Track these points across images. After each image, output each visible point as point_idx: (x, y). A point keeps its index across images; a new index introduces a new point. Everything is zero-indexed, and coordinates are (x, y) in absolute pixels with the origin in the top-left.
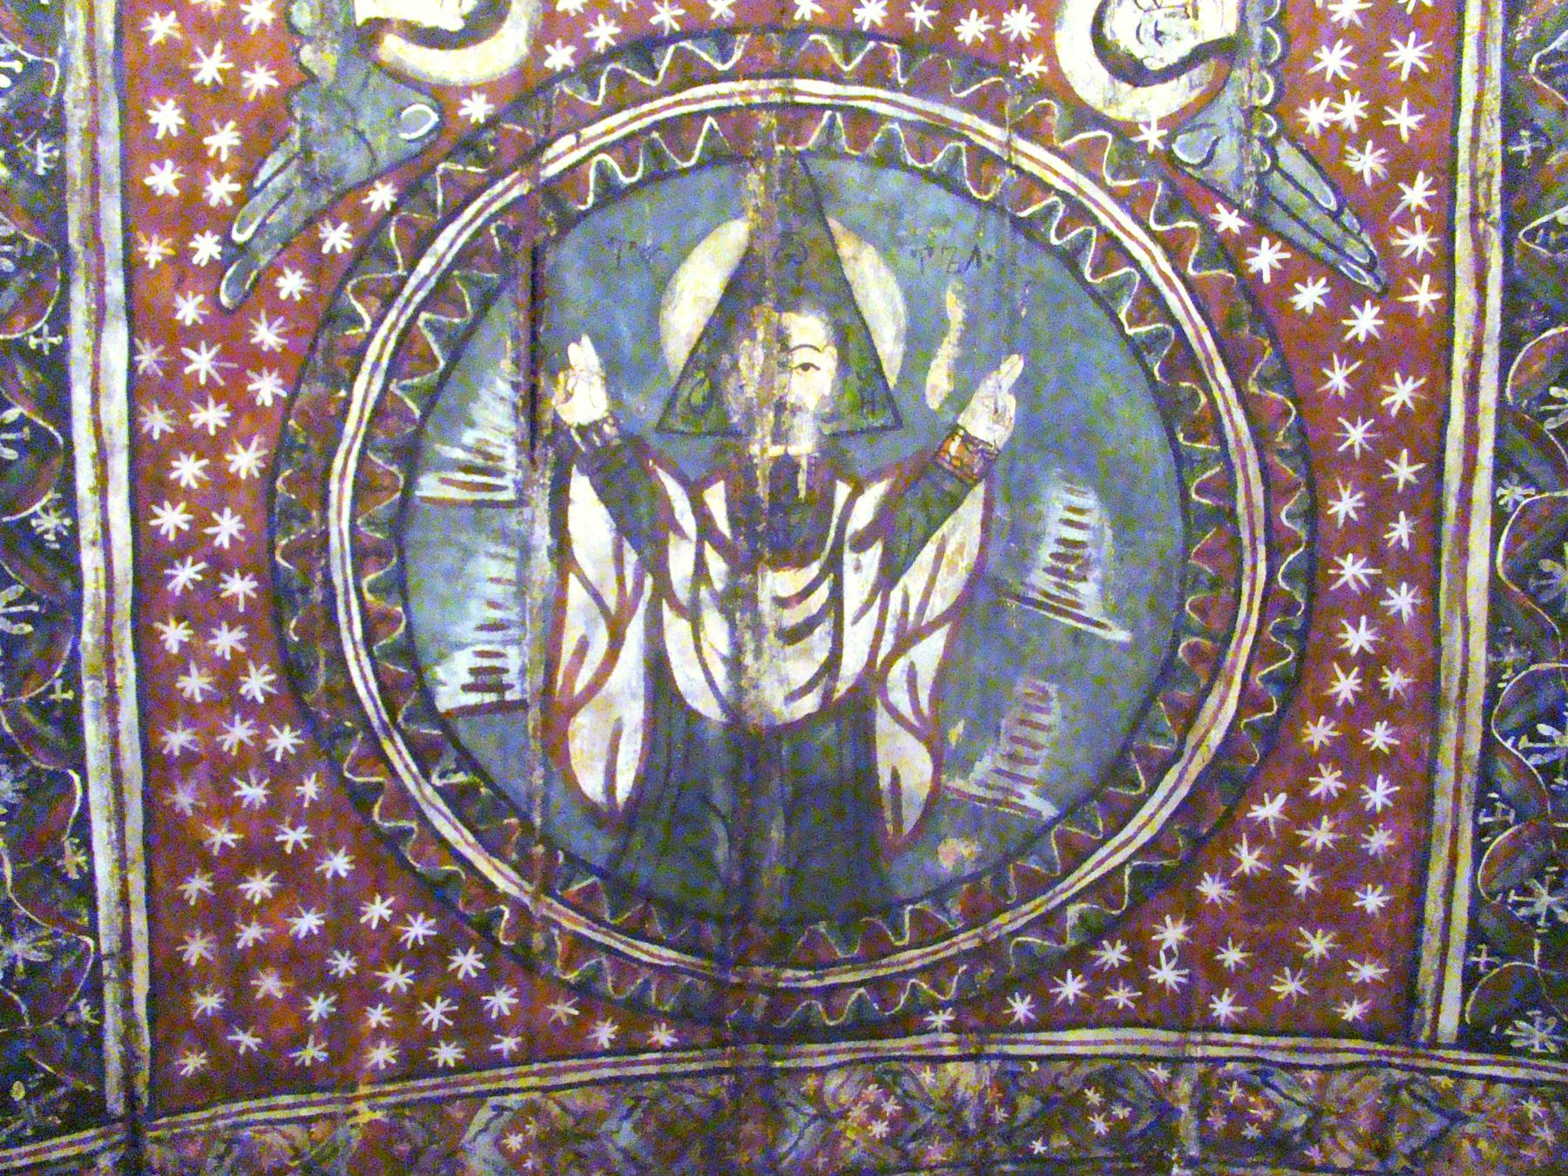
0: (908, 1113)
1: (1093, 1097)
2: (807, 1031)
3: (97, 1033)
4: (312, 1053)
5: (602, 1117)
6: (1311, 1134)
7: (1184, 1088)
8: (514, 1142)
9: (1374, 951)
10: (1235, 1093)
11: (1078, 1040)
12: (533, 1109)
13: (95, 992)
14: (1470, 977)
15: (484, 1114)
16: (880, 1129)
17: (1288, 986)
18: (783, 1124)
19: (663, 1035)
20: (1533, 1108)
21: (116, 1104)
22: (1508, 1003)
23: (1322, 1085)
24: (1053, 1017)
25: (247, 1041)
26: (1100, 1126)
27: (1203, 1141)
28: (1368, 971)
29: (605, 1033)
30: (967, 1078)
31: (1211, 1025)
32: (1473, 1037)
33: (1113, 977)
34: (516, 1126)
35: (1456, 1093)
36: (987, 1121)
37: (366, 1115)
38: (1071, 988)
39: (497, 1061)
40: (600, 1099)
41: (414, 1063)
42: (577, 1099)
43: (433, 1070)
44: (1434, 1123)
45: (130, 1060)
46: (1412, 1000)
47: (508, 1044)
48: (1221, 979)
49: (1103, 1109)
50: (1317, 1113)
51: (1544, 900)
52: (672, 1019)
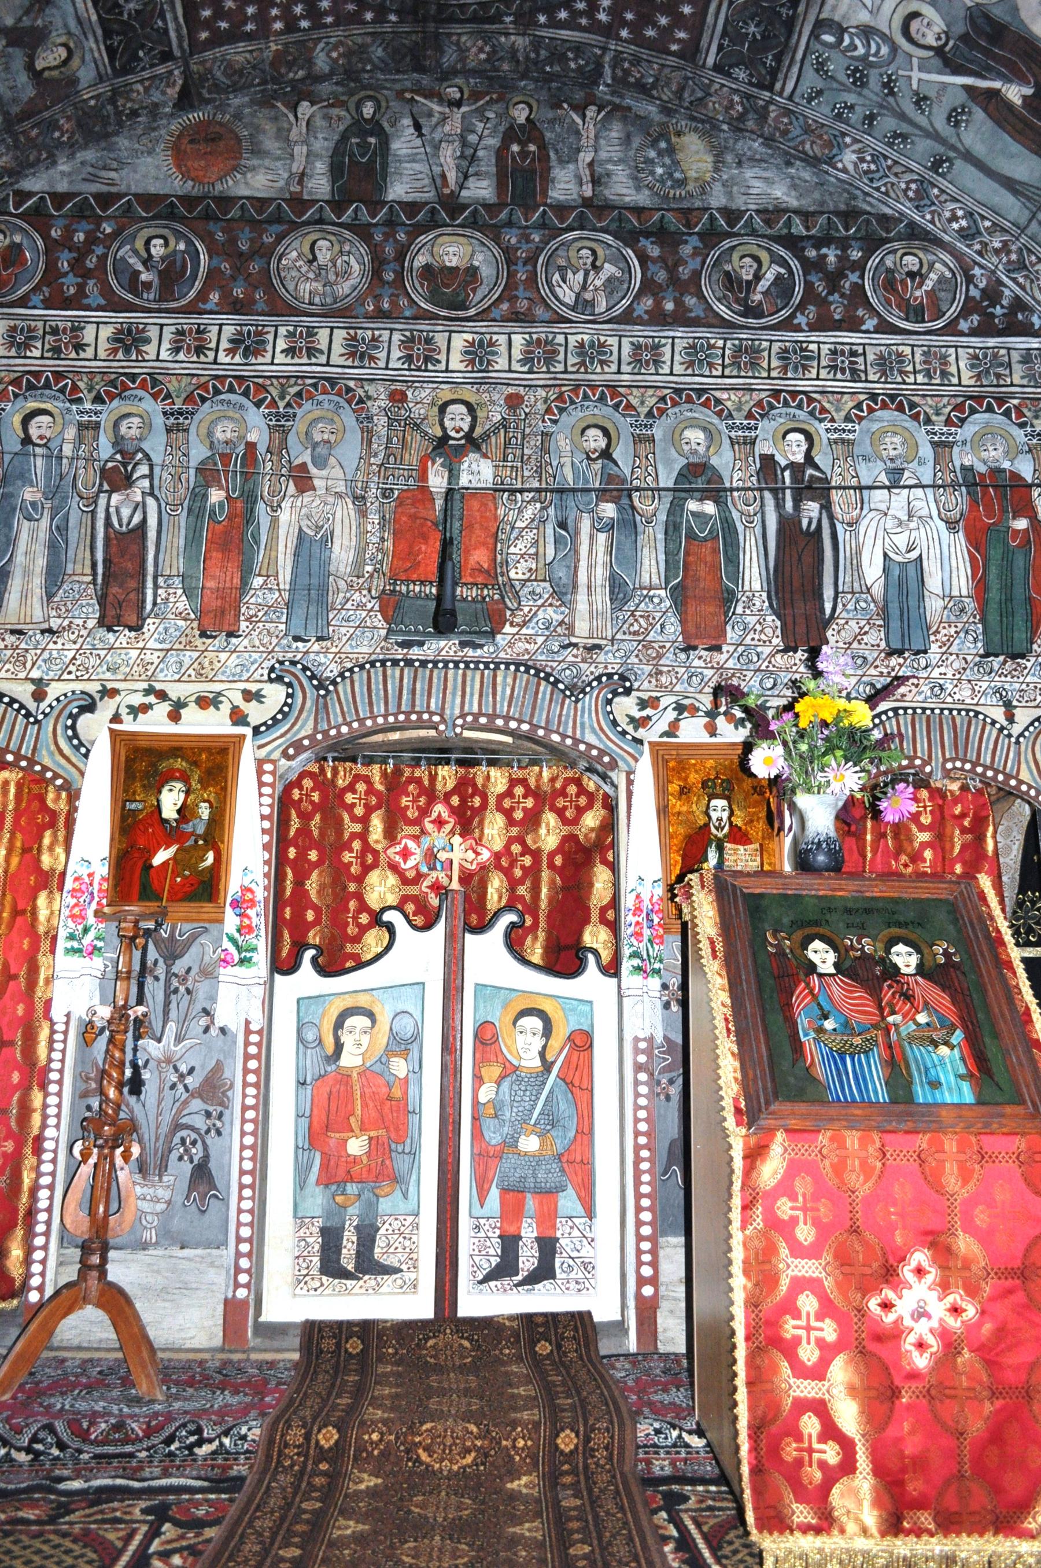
0: (494, 52)
1: (570, 55)
2: (452, 20)
3: (166, 31)
4: (250, 27)
5: (368, 46)
6: (654, 86)
7: (607, 59)
8: (334, 55)
9: (686, 30)
10: (626, 65)
11: (565, 34)
12: (341, 43)
13: (162, 16)
14: (720, 47)
15: (322, 45)
16: (483, 56)
17: (650, 33)
18: (442, 52)
19: (393, 18)
20: (736, 99)
21: (177, 53)
22: (733, 60)
23: (660, 70)
24: (554, 23)
25: (224, 25)
26: (573, 65)
27: (613, 79)
28: (682, 35)
29: (369, 16)
30: (521, 42)
31: (619, 39)
32: (717, 68)
33: (581, 13)
34: (335, 48)
35: (709, 86)
36: (527, 58)
37: (274, 47)
38: (563, 15)
39: (325, 26)
40: (369, 40)
41: (291, 26)
42: (359, 40)
43: (299, 30)
44: (700, 94)
45: (180, 38)
46: (697, 49)
47: (329, 20)
48: (624, 23)
49: (575, 59)
50: (657, 80)
51: (752, 29)
52: (397, 12)
